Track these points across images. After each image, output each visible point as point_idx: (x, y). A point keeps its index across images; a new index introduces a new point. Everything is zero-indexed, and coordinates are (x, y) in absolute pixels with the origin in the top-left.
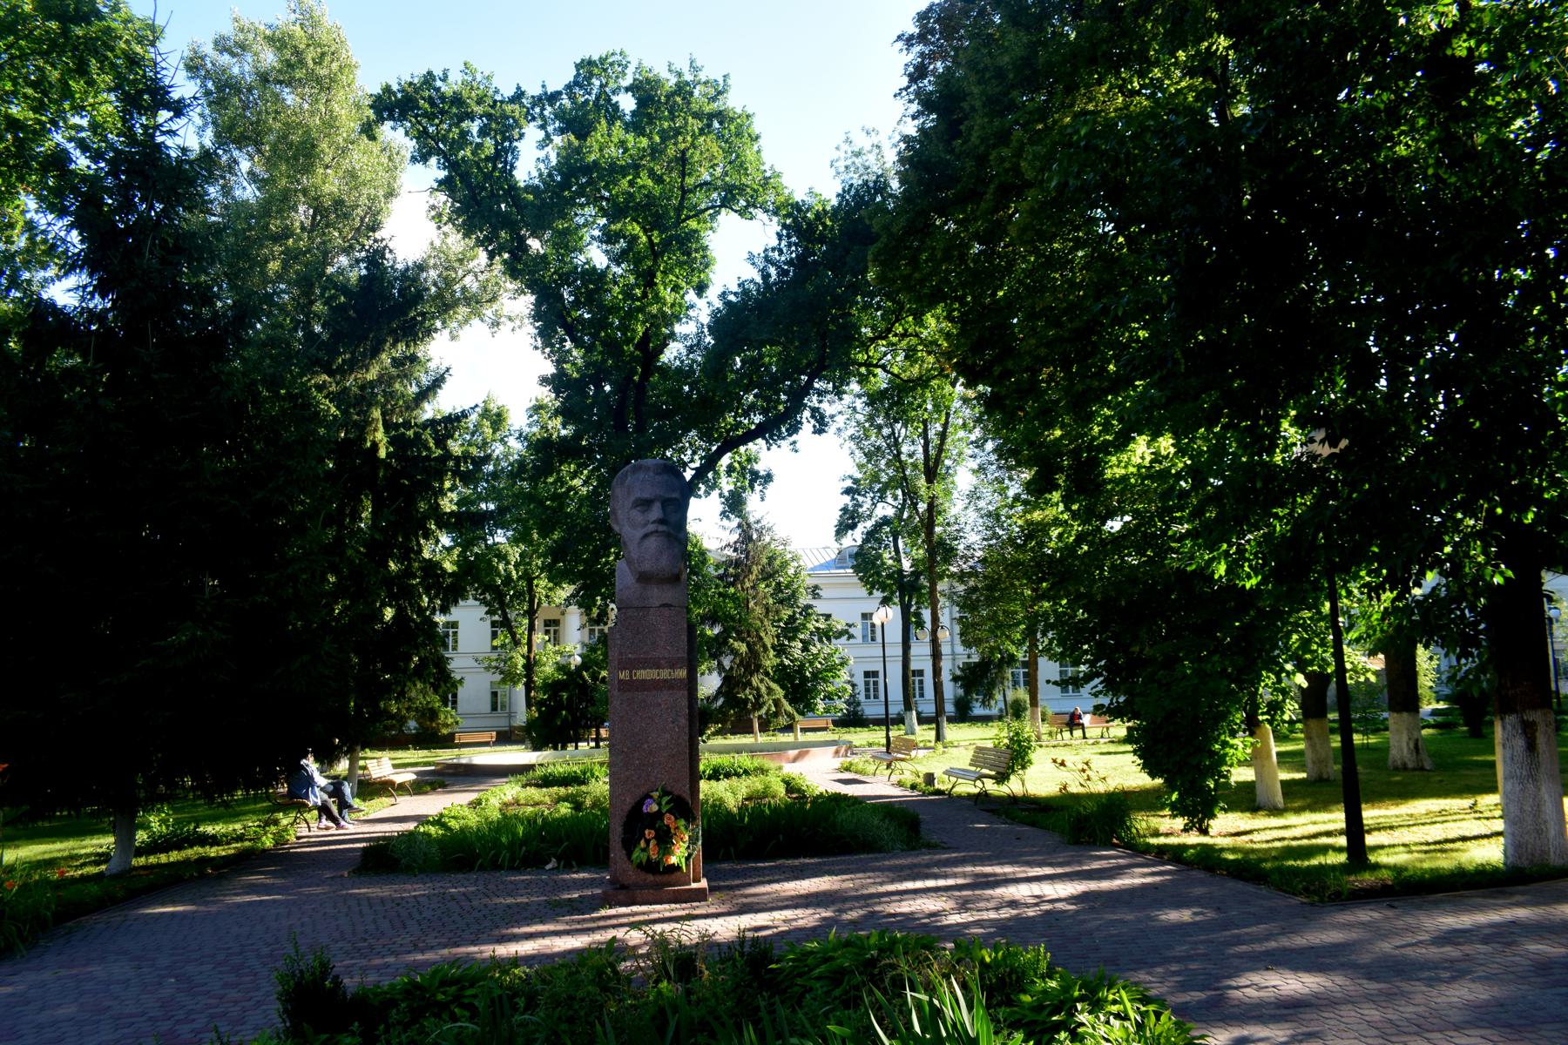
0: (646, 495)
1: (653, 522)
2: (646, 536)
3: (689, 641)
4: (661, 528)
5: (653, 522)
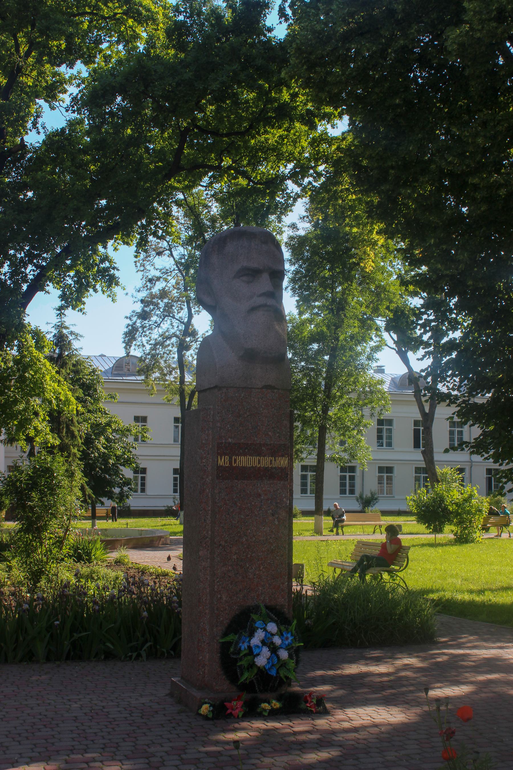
0: (254, 265)
2: (253, 309)
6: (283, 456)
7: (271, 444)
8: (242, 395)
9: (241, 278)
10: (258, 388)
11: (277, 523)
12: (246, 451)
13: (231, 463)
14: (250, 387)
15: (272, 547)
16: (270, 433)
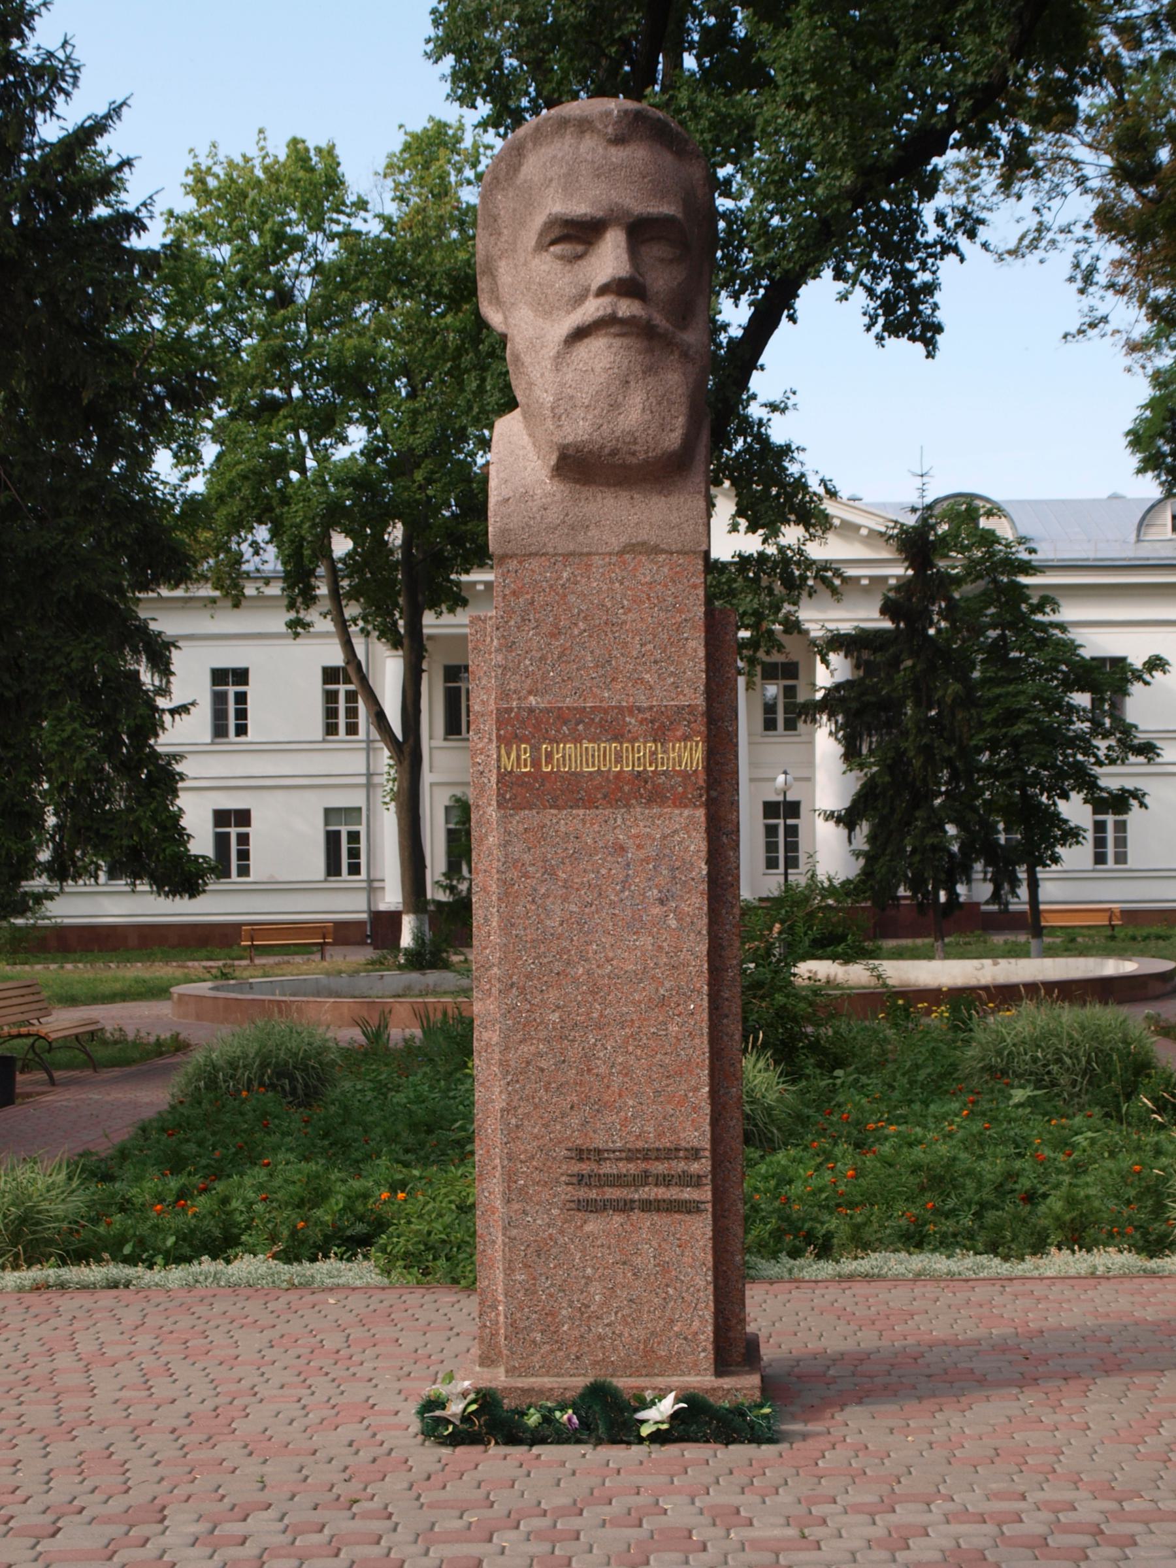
0: (580, 208)
1: (603, 291)
2: (579, 334)
3: (709, 658)
4: (626, 308)
5: (603, 291)
6: (686, 738)
7: (651, 708)
8: (565, 575)
9: (552, 249)
10: (610, 554)
11: (673, 923)
12: (581, 727)
13: (536, 763)
14: (585, 550)
15: (662, 991)
16: (647, 676)
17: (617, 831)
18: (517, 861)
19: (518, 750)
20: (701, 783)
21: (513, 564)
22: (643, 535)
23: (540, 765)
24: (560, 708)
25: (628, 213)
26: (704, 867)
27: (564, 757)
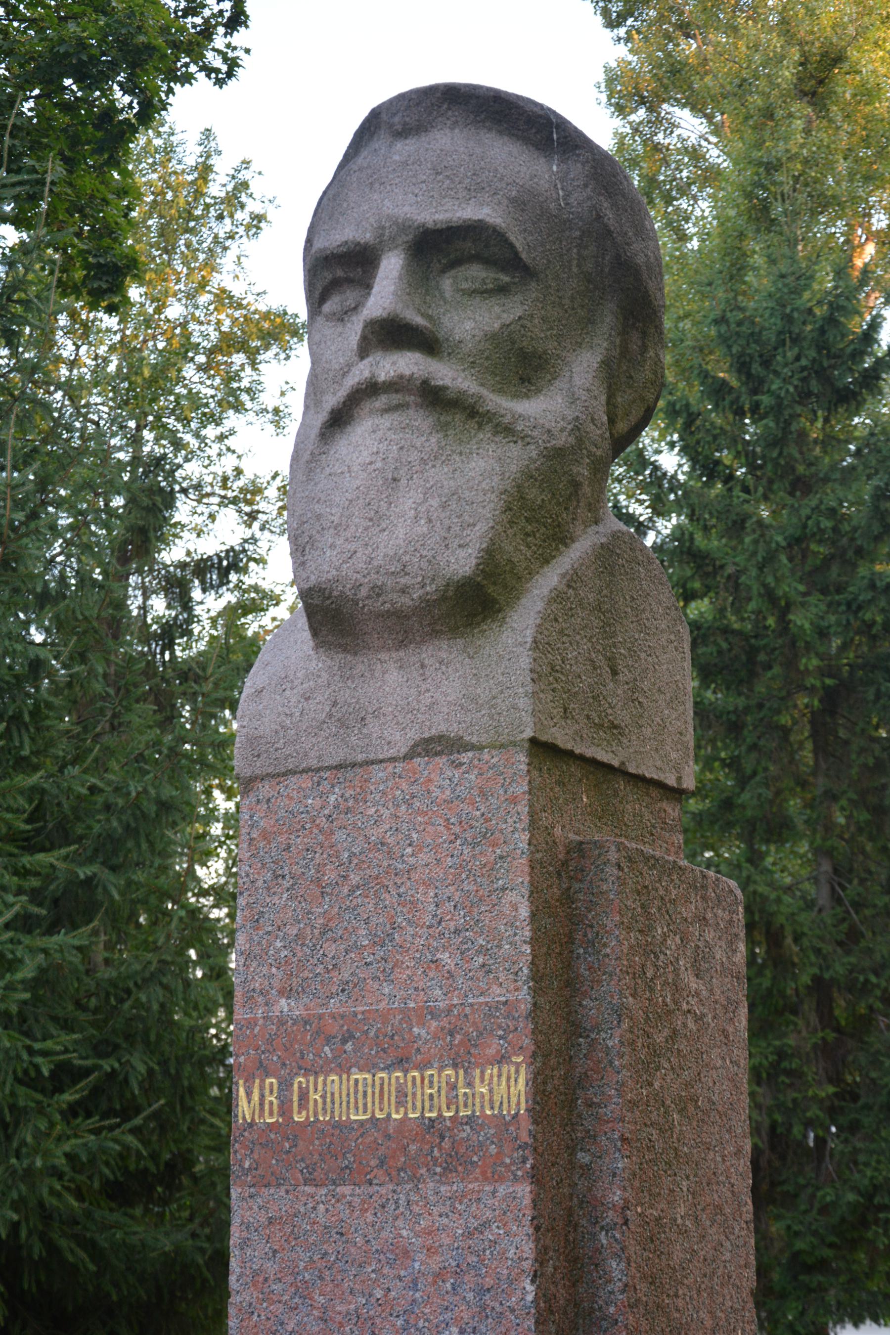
6: (502, 1059)
7: (449, 1010)
10: (393, 760)
12: (349, 1046)
13: (285, 1109)
14: (360, 758)
16: (444, 956)
17: (400, 1223)
18: (256, 1273)
19: (262, 1088)
20: (525, 1137)
21: (265, 789)
22: (439, 726)
23: (291, 1111)
24: (321, 1017)
25: (403, 227)
26: (530, 1288)
27: (324, 1097)
